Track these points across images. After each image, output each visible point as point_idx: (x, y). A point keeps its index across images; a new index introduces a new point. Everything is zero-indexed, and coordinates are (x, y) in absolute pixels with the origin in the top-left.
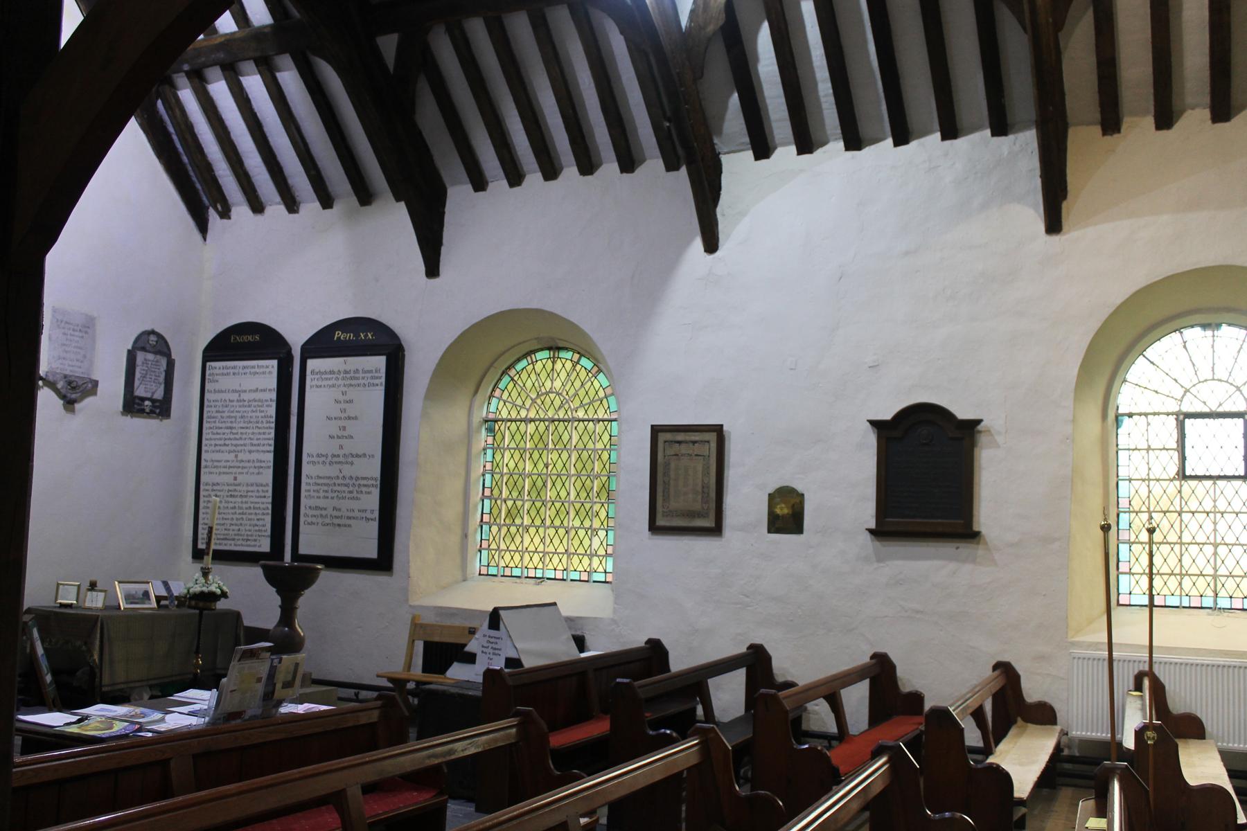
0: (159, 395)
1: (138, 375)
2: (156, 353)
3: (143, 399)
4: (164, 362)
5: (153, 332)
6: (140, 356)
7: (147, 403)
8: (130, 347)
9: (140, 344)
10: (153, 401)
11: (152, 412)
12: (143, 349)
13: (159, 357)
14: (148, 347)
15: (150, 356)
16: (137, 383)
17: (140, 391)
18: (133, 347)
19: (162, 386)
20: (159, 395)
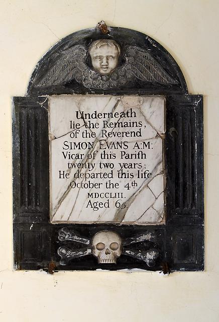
0: (148, 206)
1: (58, 162)
2: (119, 91)
3: (88, 230)
4: (152, 112)
5: (102, 34)
6: (61, 112)
7: (100, 238)
8: (22, 91)
9: (58, 75)
10: (127, 232)
11: (123, 263)
12: (74, 87)
13: (131, 101)
14: (88, 83)
15: (100, 104)
16: (57, 185)
17: (69, 206)
18: (31, 88)
19: (158, 184)
20: (148, 206)
